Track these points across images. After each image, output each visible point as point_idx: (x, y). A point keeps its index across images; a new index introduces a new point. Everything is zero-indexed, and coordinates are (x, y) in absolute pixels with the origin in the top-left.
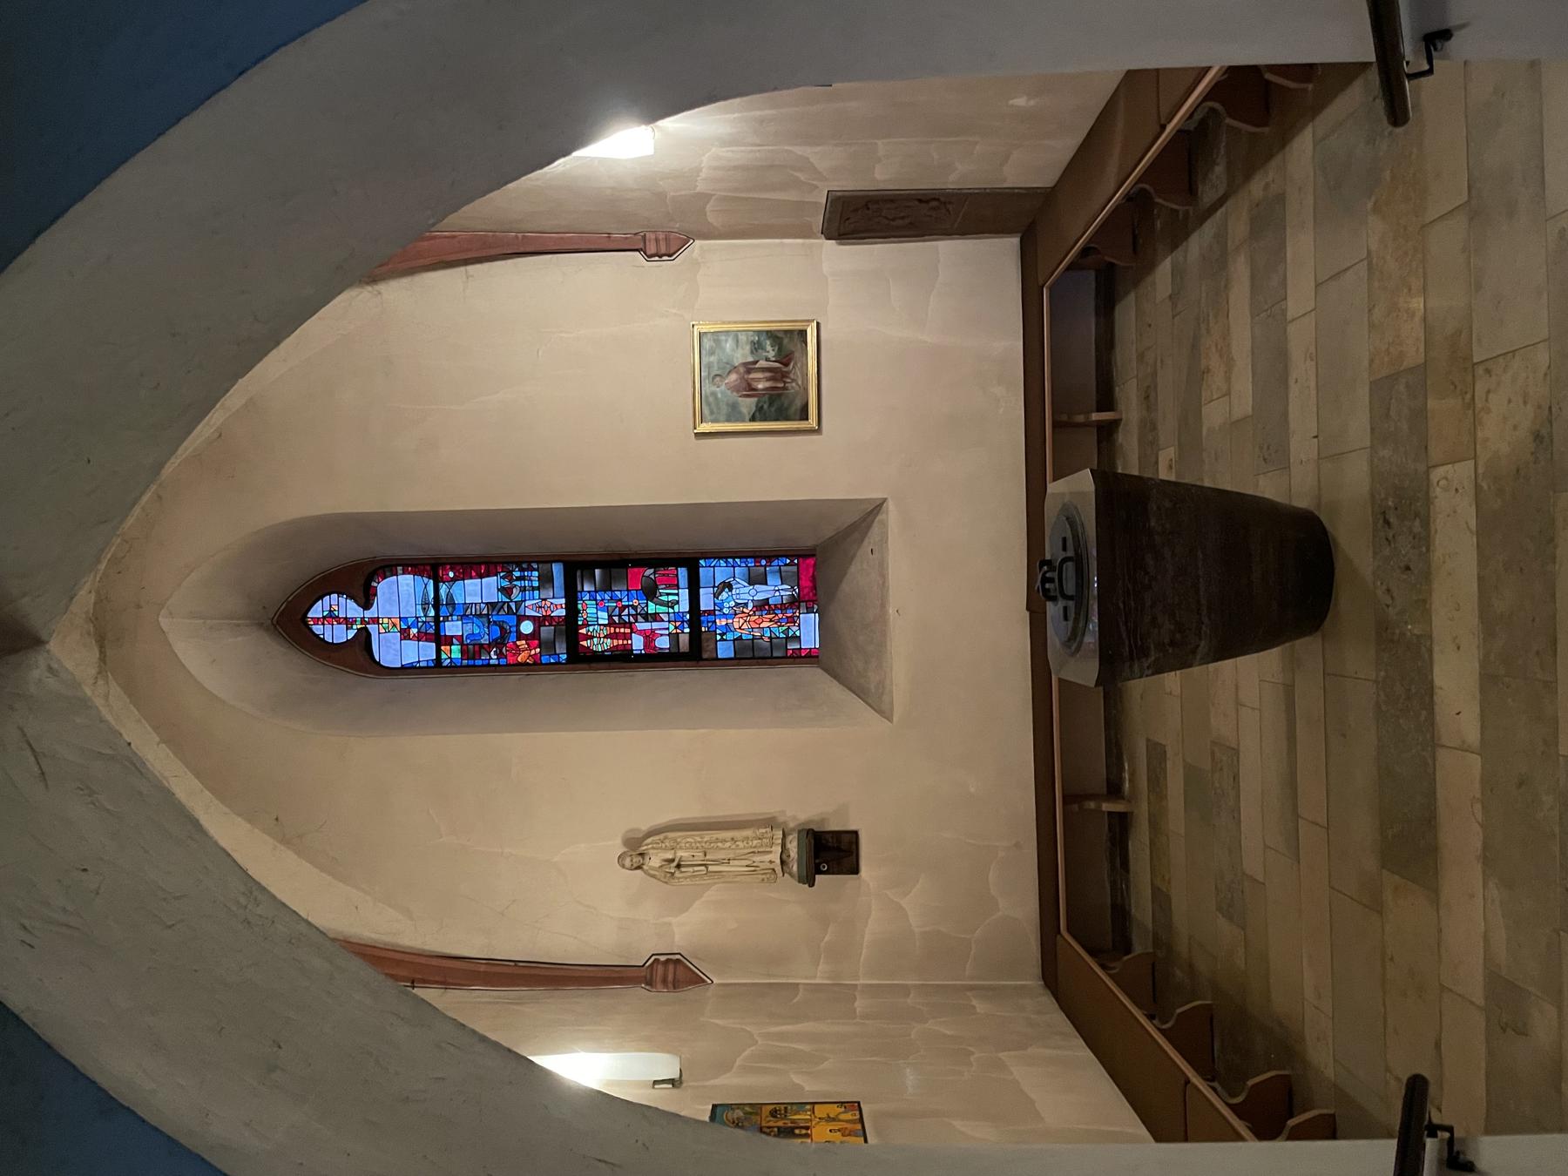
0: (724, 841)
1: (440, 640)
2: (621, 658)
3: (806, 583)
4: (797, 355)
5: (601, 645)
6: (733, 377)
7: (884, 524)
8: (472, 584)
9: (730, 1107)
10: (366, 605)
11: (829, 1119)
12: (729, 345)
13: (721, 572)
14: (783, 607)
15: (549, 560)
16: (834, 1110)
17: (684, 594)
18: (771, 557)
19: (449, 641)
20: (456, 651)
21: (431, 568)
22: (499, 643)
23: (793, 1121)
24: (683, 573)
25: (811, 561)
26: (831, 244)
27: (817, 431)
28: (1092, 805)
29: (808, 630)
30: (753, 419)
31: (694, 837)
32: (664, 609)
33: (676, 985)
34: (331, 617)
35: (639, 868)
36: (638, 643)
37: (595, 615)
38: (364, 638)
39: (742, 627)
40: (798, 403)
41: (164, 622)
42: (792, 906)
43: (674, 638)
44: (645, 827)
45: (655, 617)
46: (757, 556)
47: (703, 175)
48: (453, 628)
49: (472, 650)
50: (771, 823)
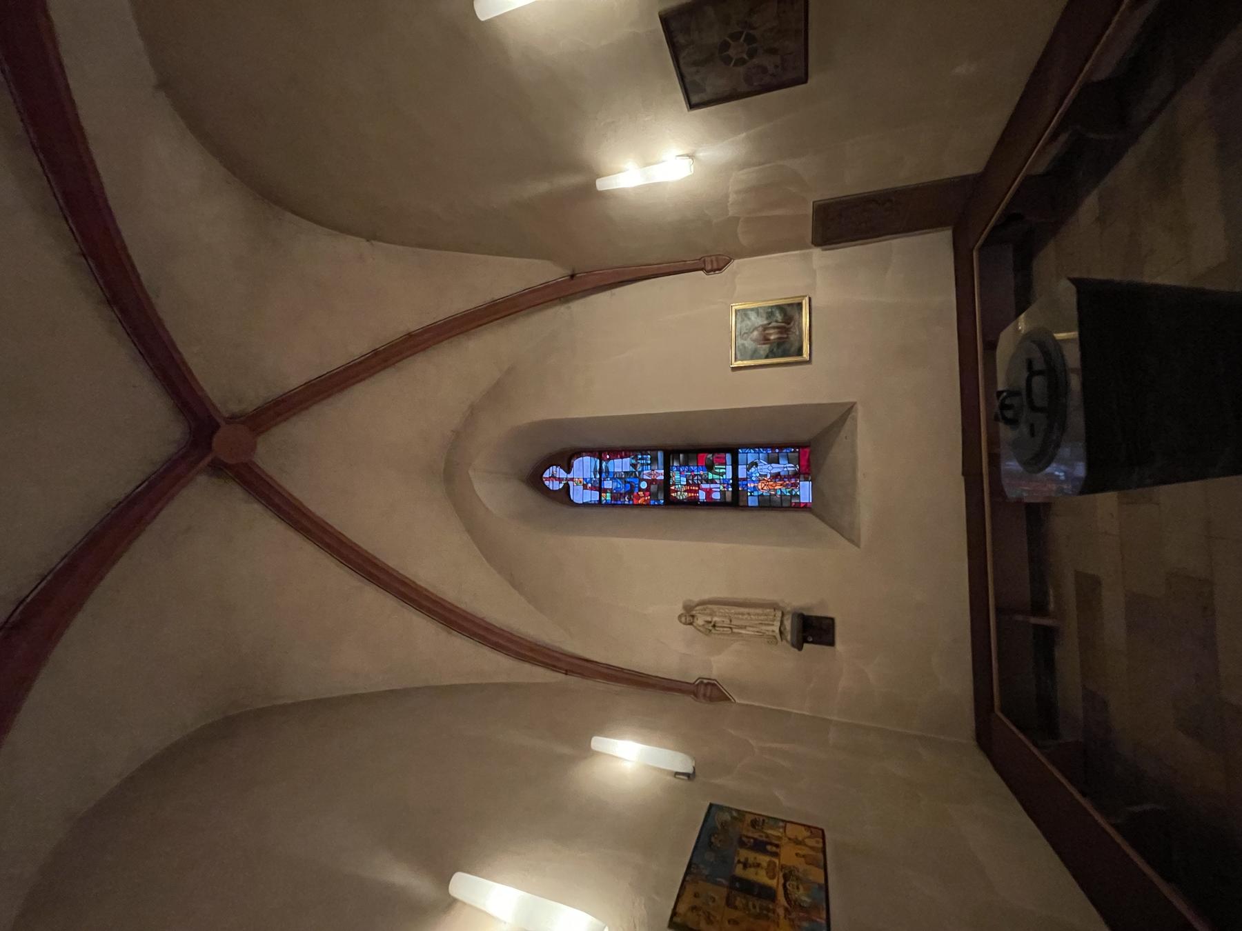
0: (743, 614)
1: (601, 490)
2: (693, 503)
3: (804, 463)
4: (797, 316)
5: (682, 496)
6: (756, 333)
7: (855, 419)
8: (618, 461)
9: (721, 808)
10: (568, 472)
11: (797, 842)
12: (753, 316)
13: (751, 457)
14: (789, 477)
15: (654, 449)
16: (802, 834)
17: (729, 468)
18: (781, 447)
19: (605, 491)
20: (608, 497)
21: (599, 453)
22: (630, 492)
23: (767, 836)
24: (728, 457)
25: (807, 450)
26: (817, 252)
27: (809, 362)
28: (1020, 618)
29: (805, 492)
30: (767, 357)
31: (726, 609)
32: (716, 477)
33: (711, 699)
34: (553, 477)
35: (691, 624)
36: (702, 496)
37: (679, 479)
38: (567, 488)
39: (764, 489)
40: (797, 345)
41: (471, 473)
42: (785, 663)
43: (723, 493)
44: (696, 599)
45: (713, 481)
46: (773, 447)
47: (730, 199)
48: (608, 484)
49: (616, 495)
50: (774, 606)
